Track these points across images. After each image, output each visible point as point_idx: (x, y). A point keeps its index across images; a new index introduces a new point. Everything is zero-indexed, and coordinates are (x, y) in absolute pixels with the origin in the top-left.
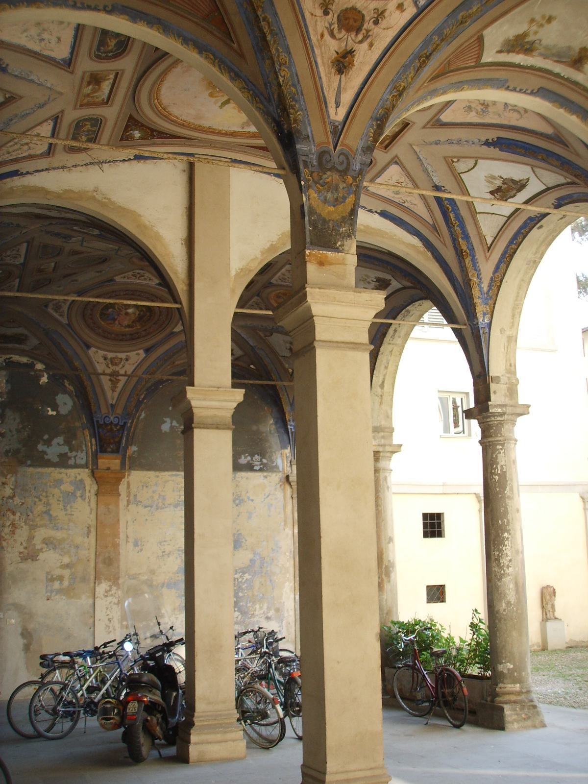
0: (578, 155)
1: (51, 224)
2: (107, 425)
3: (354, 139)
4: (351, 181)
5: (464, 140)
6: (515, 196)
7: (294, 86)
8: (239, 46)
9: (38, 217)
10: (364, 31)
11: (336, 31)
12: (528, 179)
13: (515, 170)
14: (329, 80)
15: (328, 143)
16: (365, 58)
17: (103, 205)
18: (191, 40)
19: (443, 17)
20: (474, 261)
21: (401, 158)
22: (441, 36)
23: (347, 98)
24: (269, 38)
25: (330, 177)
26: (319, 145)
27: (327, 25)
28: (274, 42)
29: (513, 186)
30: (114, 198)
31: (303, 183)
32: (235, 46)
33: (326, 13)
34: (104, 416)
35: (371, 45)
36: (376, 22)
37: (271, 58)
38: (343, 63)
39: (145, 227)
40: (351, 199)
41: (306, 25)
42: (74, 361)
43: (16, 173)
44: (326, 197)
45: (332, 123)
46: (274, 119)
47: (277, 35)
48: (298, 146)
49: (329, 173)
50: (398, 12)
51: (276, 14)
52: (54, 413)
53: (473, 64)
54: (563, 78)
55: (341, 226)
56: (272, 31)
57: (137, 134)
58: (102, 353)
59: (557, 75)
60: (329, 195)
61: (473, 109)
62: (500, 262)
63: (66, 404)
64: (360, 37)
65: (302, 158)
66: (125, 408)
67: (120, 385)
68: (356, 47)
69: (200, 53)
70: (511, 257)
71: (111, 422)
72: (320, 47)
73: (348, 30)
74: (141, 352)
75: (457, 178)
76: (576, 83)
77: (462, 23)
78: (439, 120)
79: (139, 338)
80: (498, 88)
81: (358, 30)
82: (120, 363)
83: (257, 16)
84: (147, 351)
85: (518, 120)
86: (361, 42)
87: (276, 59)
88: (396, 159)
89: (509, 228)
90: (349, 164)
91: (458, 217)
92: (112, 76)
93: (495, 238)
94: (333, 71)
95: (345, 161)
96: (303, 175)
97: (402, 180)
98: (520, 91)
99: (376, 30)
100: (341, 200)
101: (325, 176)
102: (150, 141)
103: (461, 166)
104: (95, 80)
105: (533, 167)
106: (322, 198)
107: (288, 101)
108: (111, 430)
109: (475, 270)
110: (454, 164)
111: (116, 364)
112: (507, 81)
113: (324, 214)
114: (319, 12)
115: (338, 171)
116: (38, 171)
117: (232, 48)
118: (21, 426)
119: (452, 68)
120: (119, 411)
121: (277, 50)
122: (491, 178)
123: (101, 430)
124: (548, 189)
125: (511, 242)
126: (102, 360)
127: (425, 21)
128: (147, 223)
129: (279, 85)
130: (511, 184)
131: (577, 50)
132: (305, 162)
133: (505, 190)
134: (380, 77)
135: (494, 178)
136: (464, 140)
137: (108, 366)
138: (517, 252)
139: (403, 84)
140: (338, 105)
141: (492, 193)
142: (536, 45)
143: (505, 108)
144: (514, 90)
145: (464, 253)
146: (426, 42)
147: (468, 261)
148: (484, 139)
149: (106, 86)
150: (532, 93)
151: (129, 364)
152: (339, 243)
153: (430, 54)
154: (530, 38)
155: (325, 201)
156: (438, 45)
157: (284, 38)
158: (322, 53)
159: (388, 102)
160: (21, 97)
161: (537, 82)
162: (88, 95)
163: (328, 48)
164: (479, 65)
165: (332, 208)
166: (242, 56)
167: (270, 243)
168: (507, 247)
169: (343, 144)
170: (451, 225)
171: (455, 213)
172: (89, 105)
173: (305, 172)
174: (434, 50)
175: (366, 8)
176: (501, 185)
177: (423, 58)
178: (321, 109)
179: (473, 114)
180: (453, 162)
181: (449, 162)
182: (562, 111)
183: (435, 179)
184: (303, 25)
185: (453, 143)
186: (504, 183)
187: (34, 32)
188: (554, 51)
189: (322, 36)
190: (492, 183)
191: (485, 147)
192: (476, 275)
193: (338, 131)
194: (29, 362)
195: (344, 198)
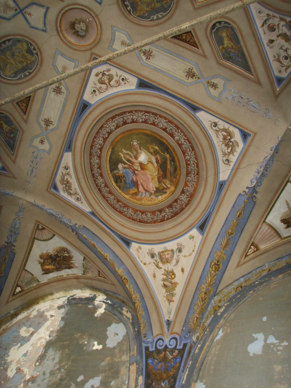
2: (158, 351)
34: (156, 339)
42: (117, 269)
52: (100, 347)
58: (146, 248)
63: (117, 334)
66: (186, 322)
67: (178, 291)
71: (166, 346)
74: (195, 232)
79: (182, 209)
82: (172, 257)
84: (202, 228)
108: (165, 359)
111: (167, 261)
118: (58, 366)
120: (177, 328)
123: (150, 361)
126: (148, 259)
137: (157, 266)
151: (185, 256)
194: (91, 296)
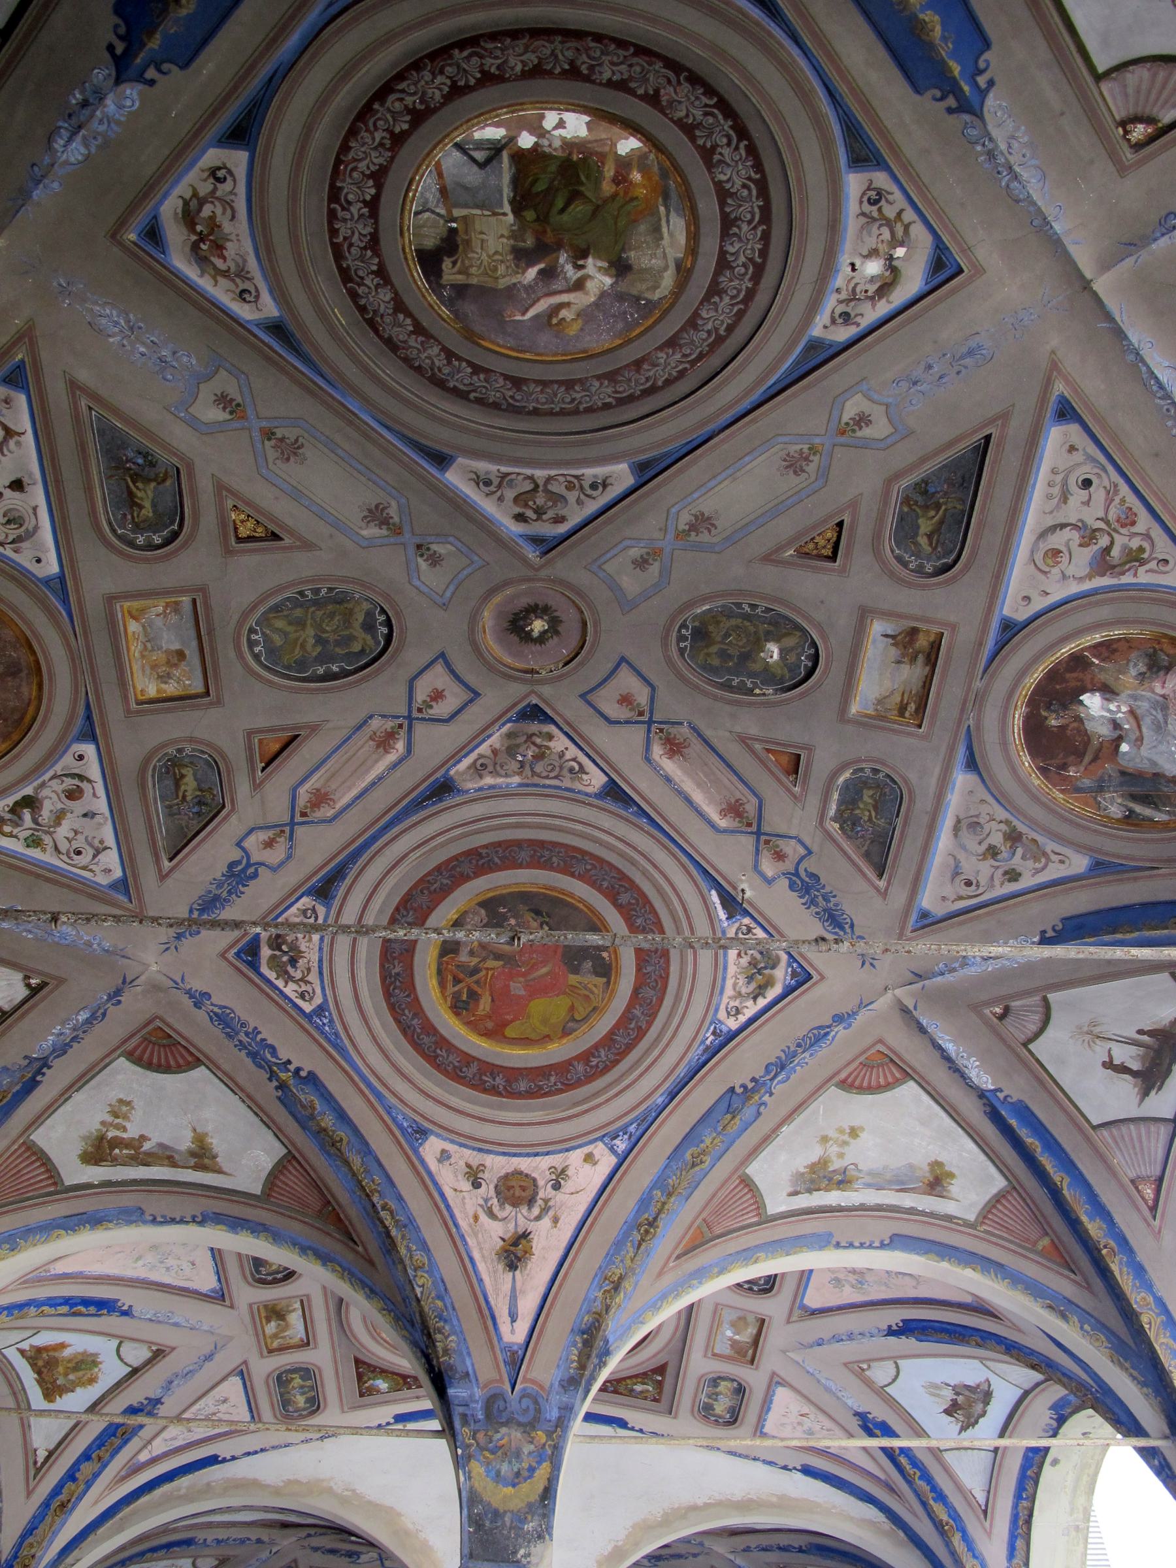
1: (309, 1535)
3: (545, 1368)
4: (543, 1440)
7: (439, 1297)
8: (366, 1249)
9: (285, 1525)
10: (540, 1202)
11: (496, 1209)
13: (965, 1368)
14: (496, 1282)
15: (501, 1380)
16: (548, 1241)
17: (344, 1501)
18: (310, 1248)
19: (662, 1161)
20: (965, 1537)
21: (782, 1374)
22: (665, 1189)
23: (528, 1305)
24: (394, 1232)
25: (510, 1436)
26: (485, 1386)
27: (482, 1202)
28: (403, 1237)
30: (361, 1489)
31: (459, 1451)
32: (360, 1249)
33: (476, 1185)
35: (556, 1220)
36: (557, 1186)
37: (401, 1261)
38: (514, 1253)
39: (407, 1533)
40: (544, 1470)
41: (448, 1206)
43: (213, 1460)
44: (498, 1473)
45: (508, 1348)
46: (422, 1351)
47: (405, 1226)
48: (451, 1392)
49: (504, 1430)
50: (587, 1166)
51: (400, 1198)
53: (755, 1219)
54: (923, 1213)
55: (524, 1521)
56: (397, 1221)
57: (383, 1385)
59: (912, 1211)
60: (505, 1468)
64: (536, 1211)
65: (457, 1411)
68: (531, 1226)
69: (324, 1264)
72: (476, 1234)
73: (516, 1203)
75: (881, 1393)
76: (949, 1218)
77: (694, 1165)
78: (803, 1307)
80: (821, 1248)
81: (531, 1202)
83: (374, 1206)
86: (538, 1218)
87: (407, 1262)
88: (776, 1379)
90: (538, 1411)
91: (915, 1463)
92: (298, 1305)
94: (501, 1267)
95: (532, 1407)
96: (460, 1438)
97: (806, 1410)
98: (862, 1246)
99: (559, 1197)
100: (525, 1474)
101: (498, 1436)
102: (406, 1393)
103: (881, 1373)
104: (276, 1313)
105: (981, 1359)
106: (493, 1473)
107: (433, 1322)
112: (830, 1235)
113: (496, 1502)
114: (466, 1186)
115: (520, 1424)
116: (248, 1454)
117: (357, 1252)
119: (718, 1231)
121: (408, 1249)
122: (933, 1388)
124: (1026, 1393)
125: (1018, 1497)
127: (633, 1173)
128: (410, 1526)
129: (418, 1301)
131: (927, 1168)
132: (464, 1417)
133: (966, 1405)
134: (578, 1264)
135: (936, 1387)
136: (856, 1332)
138: (1035, 1513)
139: (618, 1272)
140: (513, 1317)
142: (852, 1172)
144: (851, 1245)
146: (645, 1202)
147: (956, 1540)
149: (295, 1319)
150: (882, 1246)
152: (522, 1552)
153: (655, 1219)
154: (836, 1164)
155: (498, 1477)
156: (664, 1204)
157: (417, 1229)
158: (479, 1243)
159: (598, 1303)
160: (173, 1349)
161: (885, 1228)
162: (275, 1336)
163: (487, 1236)
164: (767, 1220)
165: (509, 1490)
166: (371, 1262)
167: (613, 1544)
168: (1015, 1506)
169: (525, 1380)
171: (907, 1456)
172: (282, 1349)
173: (464, 1432)
174: (660, 1212)
175: (536, 1168)
177: (644, 1226)
178: (486, 1328)
179: (847, 1289)
181: (858, 1370)
182: (945, 1265)
183: (850, 1402)
184: (442, 1206)
186: (957, 1394)
187: (150, 1258)
188: (888, 1176)
189: (476, 1218)
190: (938, 1396)
191: (892, 1339)
193: (516, 1360)
195: (532, 1470)
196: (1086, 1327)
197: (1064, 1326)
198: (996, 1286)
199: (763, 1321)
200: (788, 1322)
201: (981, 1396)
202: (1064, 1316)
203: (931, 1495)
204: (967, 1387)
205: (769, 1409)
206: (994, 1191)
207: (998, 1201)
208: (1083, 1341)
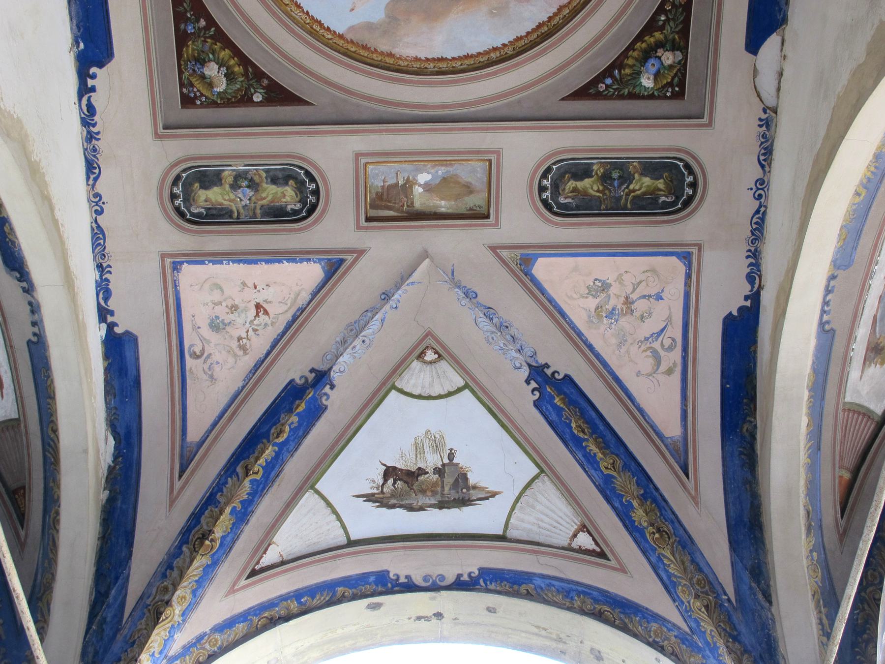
0: (695, 499)
5: (512, 331)
6: (421, 509)
12: (494, 494)
20: (209, 570)
29: (447, 489)
61: (603, 296)
62: (244, 616)
70: (273, 622)
85: (638, 374)
89: (328, 564)
93: (283, 563)
98: (826, 303)
109: (194, 592)
110: (416, 364)
124: (502, 538)
125: (298, 595)
130: (449, 480)
135: (437, 445)
136: (512, 331)
141: (390, 472)
143: (647, 339)
144: (828, 291)
145: (207, 542)
148: (542, 360)
168: (284, 598)
170: (239, 470)
171: (278, 455)
176: (430, 470)
180: (420, 356)
182: (806, 394)
183: (345, 358)
185: (491, 319)
186: (439, 471)
192: (185, 605)
196: (815, 554)
197: (804, 536)
198: (802, 453)
199: (487, 217)
200: (494, 249)
201: (454, 495)
202: (809, 528)
203: (237, 504)
204: (464, 477)
205: (294, 261)
206: (872, 407)
207: (864, 415)
208: (805, 561)
